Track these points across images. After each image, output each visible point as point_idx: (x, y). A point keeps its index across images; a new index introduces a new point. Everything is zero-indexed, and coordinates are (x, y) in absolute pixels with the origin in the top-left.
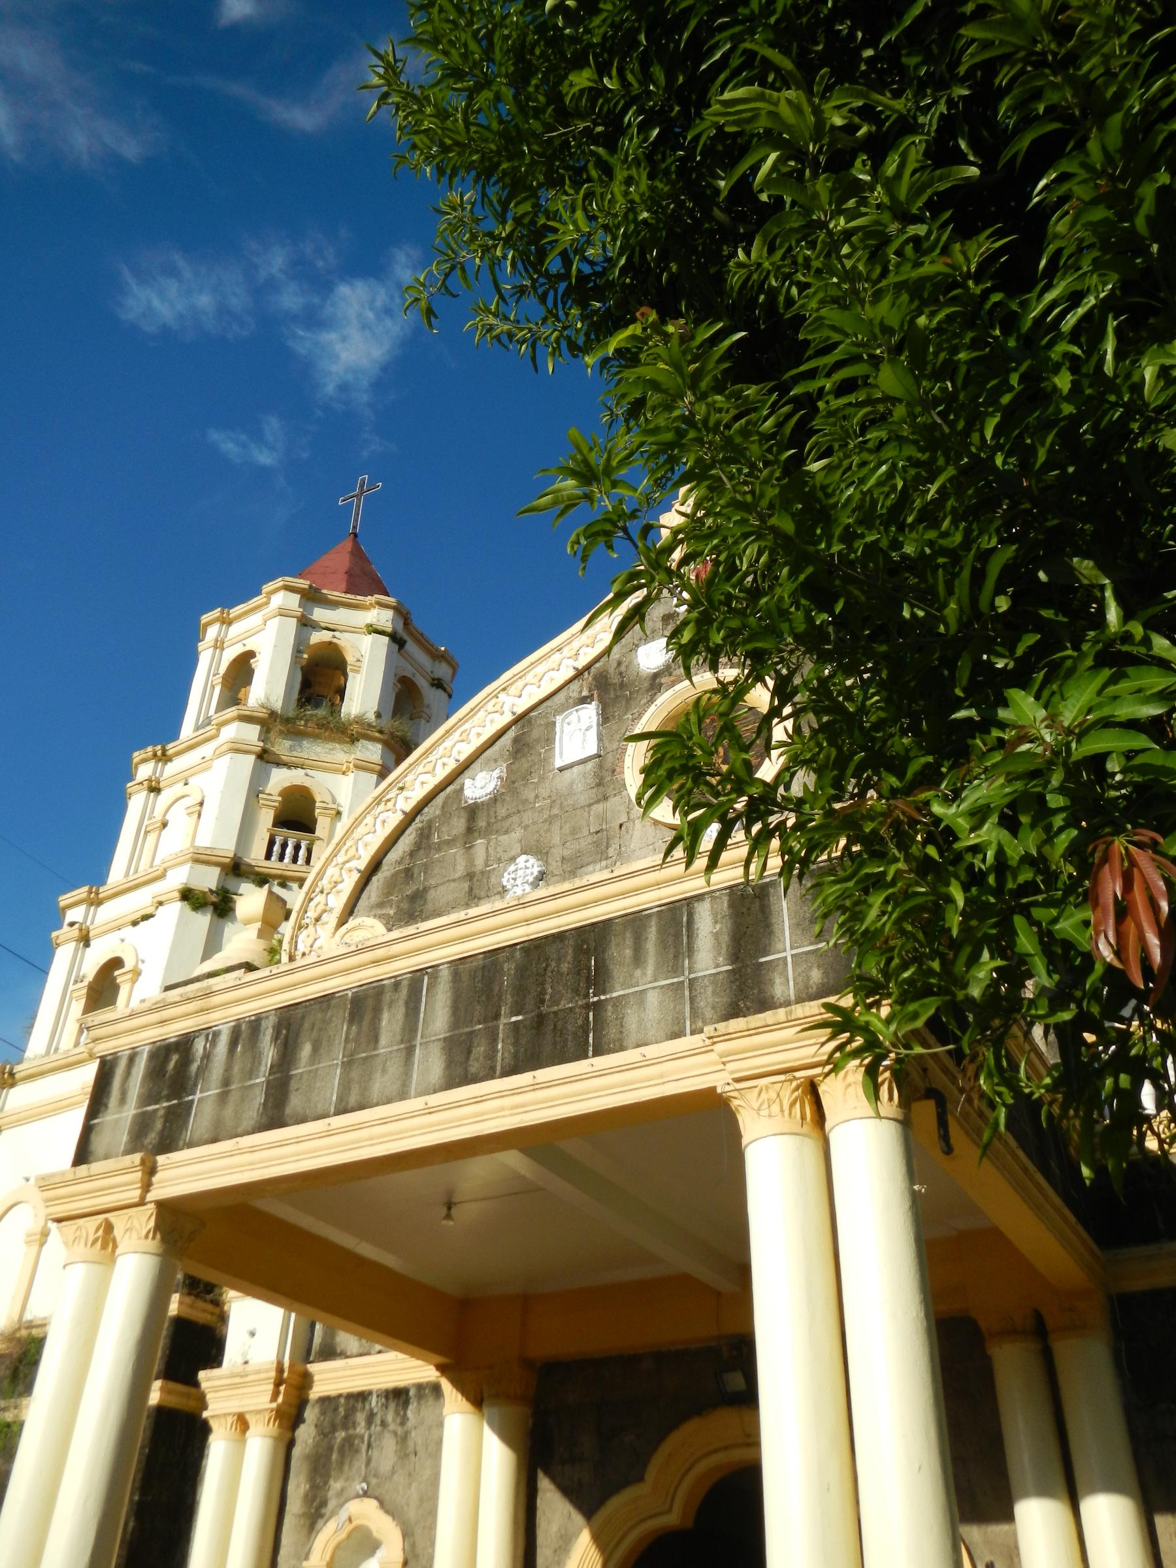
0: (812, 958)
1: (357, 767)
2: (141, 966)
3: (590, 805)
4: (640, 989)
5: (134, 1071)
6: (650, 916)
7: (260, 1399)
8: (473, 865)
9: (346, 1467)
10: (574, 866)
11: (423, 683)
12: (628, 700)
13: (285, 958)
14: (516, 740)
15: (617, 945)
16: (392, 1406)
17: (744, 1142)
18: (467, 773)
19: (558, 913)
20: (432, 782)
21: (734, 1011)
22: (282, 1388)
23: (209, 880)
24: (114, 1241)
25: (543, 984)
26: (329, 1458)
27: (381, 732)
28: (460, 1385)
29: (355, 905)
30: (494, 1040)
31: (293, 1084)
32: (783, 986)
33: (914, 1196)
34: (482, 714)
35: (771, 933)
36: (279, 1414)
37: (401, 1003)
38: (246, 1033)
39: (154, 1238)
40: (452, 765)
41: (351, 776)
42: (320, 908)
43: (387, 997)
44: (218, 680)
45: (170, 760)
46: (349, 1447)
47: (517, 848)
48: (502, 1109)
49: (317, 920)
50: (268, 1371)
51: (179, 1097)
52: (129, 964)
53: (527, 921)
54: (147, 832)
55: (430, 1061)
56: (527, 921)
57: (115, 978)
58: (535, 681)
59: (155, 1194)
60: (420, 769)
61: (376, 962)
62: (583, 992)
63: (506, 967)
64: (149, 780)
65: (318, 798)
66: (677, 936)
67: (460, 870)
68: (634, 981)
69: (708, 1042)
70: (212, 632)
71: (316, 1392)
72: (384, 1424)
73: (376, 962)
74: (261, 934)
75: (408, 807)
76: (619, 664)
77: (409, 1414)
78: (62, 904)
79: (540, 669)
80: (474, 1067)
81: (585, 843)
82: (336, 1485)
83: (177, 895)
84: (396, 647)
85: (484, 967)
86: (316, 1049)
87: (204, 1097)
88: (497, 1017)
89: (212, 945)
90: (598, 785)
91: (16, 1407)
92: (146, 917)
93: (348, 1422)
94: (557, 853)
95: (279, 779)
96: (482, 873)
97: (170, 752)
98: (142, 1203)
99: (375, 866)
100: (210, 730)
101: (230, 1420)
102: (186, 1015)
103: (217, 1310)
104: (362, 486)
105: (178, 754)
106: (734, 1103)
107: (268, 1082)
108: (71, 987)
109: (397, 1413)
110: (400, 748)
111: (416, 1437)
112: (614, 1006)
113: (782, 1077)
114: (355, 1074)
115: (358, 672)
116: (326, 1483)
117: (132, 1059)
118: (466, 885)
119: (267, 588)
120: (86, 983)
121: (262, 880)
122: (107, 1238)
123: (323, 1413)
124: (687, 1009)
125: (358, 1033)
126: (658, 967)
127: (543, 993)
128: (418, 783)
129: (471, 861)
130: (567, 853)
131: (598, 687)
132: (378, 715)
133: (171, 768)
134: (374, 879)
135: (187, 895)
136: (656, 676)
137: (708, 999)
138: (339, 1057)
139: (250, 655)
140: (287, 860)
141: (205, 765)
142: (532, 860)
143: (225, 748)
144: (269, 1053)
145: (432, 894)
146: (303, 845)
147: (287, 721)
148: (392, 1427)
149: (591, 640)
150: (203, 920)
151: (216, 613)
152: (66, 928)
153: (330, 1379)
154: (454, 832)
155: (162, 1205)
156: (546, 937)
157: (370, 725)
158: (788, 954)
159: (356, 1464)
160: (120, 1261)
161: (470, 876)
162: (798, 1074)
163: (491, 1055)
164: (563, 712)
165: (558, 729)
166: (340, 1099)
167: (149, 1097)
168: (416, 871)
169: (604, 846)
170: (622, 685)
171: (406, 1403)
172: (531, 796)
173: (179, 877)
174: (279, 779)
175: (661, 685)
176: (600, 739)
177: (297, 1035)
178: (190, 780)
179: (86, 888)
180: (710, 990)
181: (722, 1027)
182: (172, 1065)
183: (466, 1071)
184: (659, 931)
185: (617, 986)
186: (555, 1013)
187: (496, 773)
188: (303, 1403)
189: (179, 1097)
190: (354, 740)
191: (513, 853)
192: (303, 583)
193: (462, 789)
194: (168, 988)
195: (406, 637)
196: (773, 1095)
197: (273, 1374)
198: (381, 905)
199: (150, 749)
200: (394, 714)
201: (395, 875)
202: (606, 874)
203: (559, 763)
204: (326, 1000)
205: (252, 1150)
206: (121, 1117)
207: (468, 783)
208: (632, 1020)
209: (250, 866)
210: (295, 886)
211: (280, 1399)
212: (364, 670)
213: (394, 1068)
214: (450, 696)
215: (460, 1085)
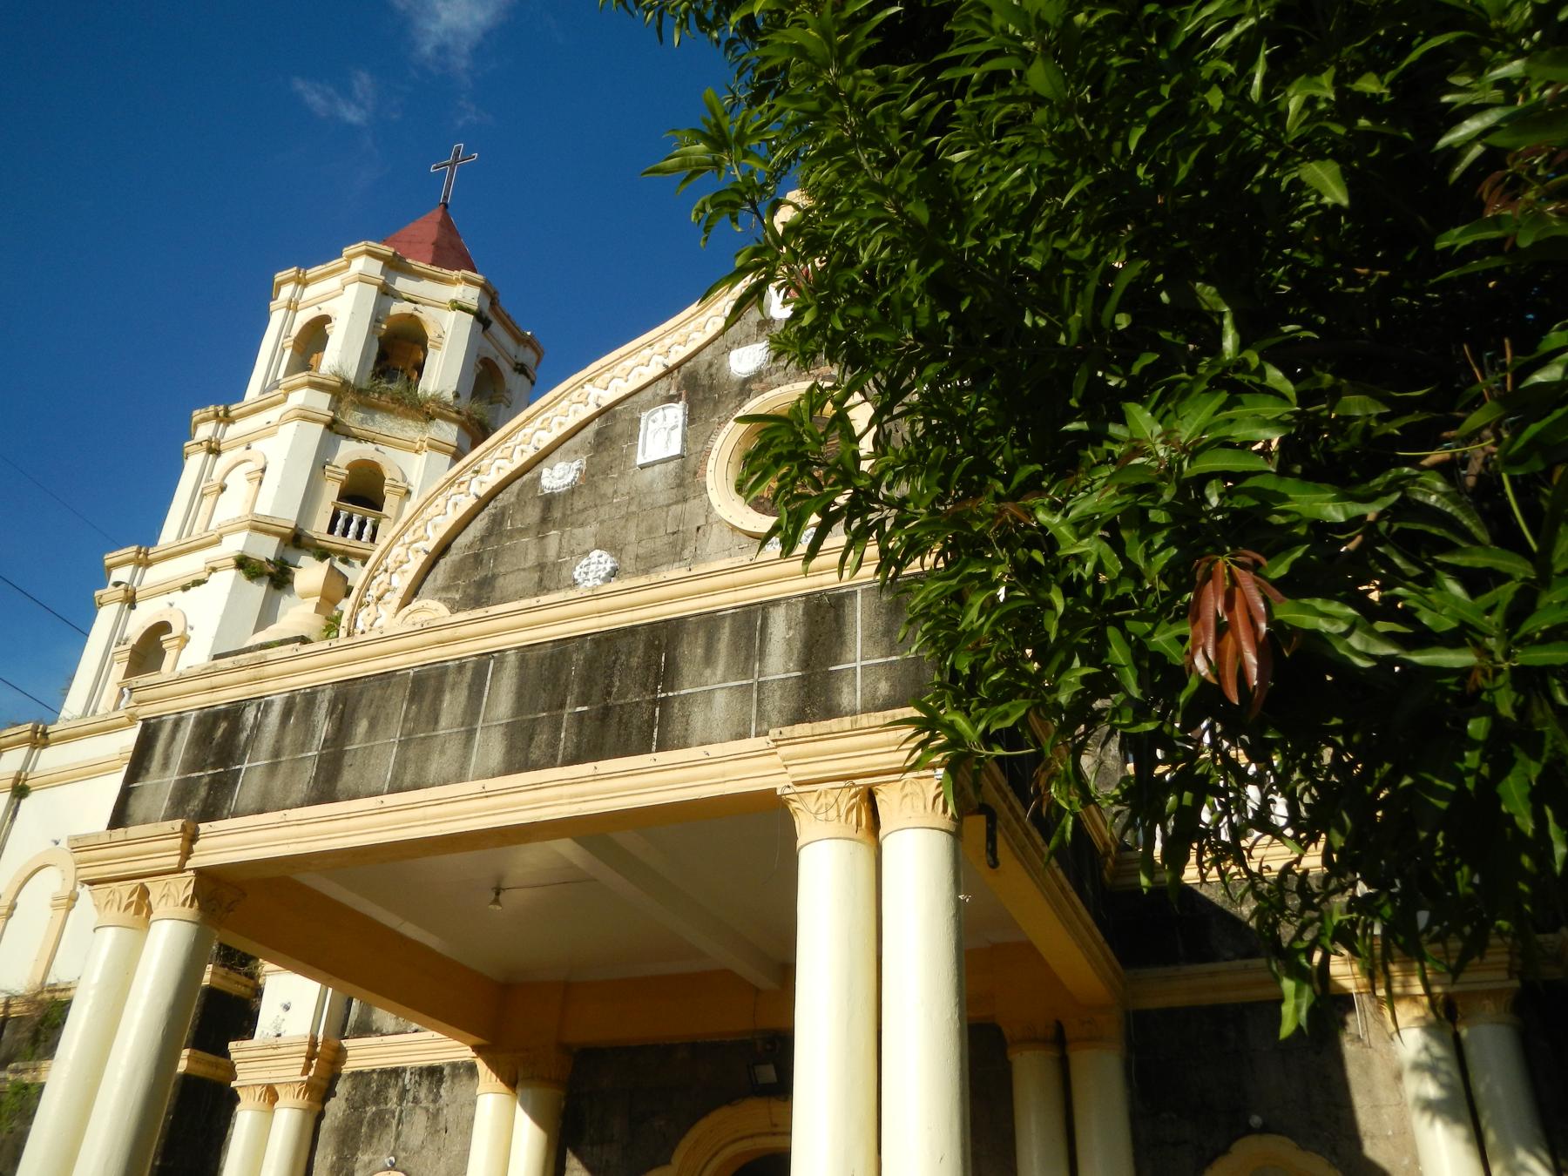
0: (881, 671)
1: (430, 446)
2: (189, 632)
3: (669, 505)
4: (710, 688)
5: (179, 736)
6: (724, 617)
7: (291, 1072)
8: (544, 555)
9: (375, 1140)
10: (648, 564)
11: (505, 367)
12: (716, 403)
13: (343, 633)
14: (598, 433)
15: (689, 644)
16: (426, 1083)
17: (799, 844)
18: (545, 462)
19: (632, 607)
20: (509, 468)
21: (799, 717)
22: (314, 1062)
23: (267, 549)
24: (149, 905)
25: (611, 676)
26: (358, 1131)
27: (458, 412)
28: (491, 1064)
29: (419, 587)
30: (558, 729)
31: (347, 760)
32: (850, 696)
33: (959, 905)
34: (565, 403)
35: (843, 643)
36: (310, 1087)
37: (465, 685)
38: (300, 705)
39: (191, 906)
40: (531, 453)
41: (425, 455)
42: (382, 588)
43: (450, 679)
44: (289, 342)
45: (233, 422)
46: (380, 1121)
47: (591, 542)
48: (561, 797)
49: (379, 599)
50: (300, 1044)
51: (226, 766)
52: (177, 630)
53: (600, 613)
54: (203, 495)
55: (489, 746)
56: (600, 613)
57: (161, 643)
58: (624, 374)
59: (195, 861)
60: (498, 454)
61: (441, 643)
62: (651, 687)
63: (575, 657)
64: (209, 441)
65: (387, 475)
66: (751, 638)
67: (532, 559)
68: (703, 680)
69: (772, 745)
70: (286, 292)
71: (350, 1066)
72: (416, 1100)
73: (441, 643)
74: (319, 609)
75: (482, 492)
76: (710, 365)
77: (442, 1091)
78: (108, 562)
79: (629, 363)
80: (535, 754)
81: (660, 542)
82: (364, 1158)
83: (232, 562)
84: (481, 327)
85: (552, 655)
87: (252, 768)
88: (562, 706)
89: (266, 616)
90: (679, 486)
91: (35, 1069)
92: (197, 583)
93: (380, 1096)
94: (632, 550)
95: (348, 452)
96: (554, 564)
97: (232, 414)
98: (181, 869)
99: (443, 548)
100: (278, 394)
101: (258, 1090)
102: (238, 683)
103: (251, 983)
104: (457, 155)
105: (242, 416)
106: (793, 805)
107: (321, 756)
108: (113, 649)
109: (430, 1090)
110: (477, 431)
111: (448, 1114)
112: (682, 703)
113: (842, 784)
114: (411, 754)
115: (438, 348)
116: (353, 1155)
117: (177, 724)
118: (536, 576)
119: (348, 251)
120: (129, 646)
121: (323, 554)
122: (142, 904)
123: (355, 1088)
124: (754, 711)
125: (419, 712)
126: (728, 667)
127: (610, 685)
128: (494, 468)
129: (543, 551)
130: (641, 551)
131: (687, 387)
132: (457, 395)
133: (233, 431)
134: (442, 562)
135: (242, 563)
136: (746, 381)
137: (776, 702)
138: (396, 735)
139: (326, 319)
140: (350, 536)
141: (270, 430)
142: (606, 556)
143: (291, 414)
145: (500, 582)
146: (369, 521)
147: (360, 391)
148: (424, 1104)
149: (682, 339)
150: (259, 590)
151: (292, 272)
152: (110, 587)
153: (363, 1054)
154: (528, 521)
155: (200, 872)
156: (618, 630)
157: (447, 405)
158: (858, 664)
159: (386, 1138)
160: (154, 926)
161: (541, 567)
162: (857, 782)
163: (553, 744)
164: (648, 408)
165: (642, 426)
166: (395, 777)
167: (193, 764)
168: (486, 557)
169: (679, 546)
170: (711, 388)
171: (440, 1081)
172: (610, 491)
173: (235, 544)
174: (348, 452)
175: (751, 391)
176: (684, 439)
177: (354, 710)
178: (253, 445)
179: (135, 548)
180: (778, 694)
181: (787, 731)
182: (220, 732)
183: (527, 758)
184: (732, 633)
185: (686, 684)
186: (621, 706)
187: (576, 465)
188: (334, 1077)
189: (226, 766)
190: (430, 418)
191: (587, 547)
192: (387, 250)
193: (539, 477)
194: (216, 657)
195: (491, 317)
196: (832, 800)
197: (306, 1048)
198: (446, 589)
199: (211, 408)
200: (474, 395)
202: (683, 572)
203: (640, 460)
204: (387, 677)
205: (300, 823)
206: (162, 782)
207: (546, 472)
208: (698, 720)
209: (311, 538)
210: (357, 563)
211: (311, 1073)
212: (445, 347)
213: (453, 749)
214: (533, 383)
215: (520, 771)
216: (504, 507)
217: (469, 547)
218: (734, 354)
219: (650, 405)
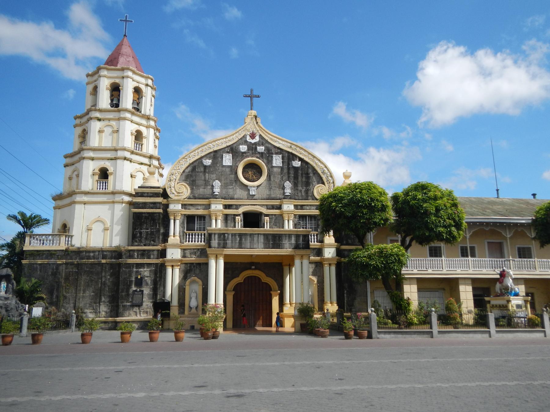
14: (214, 155)
38: (234, 235)
55: (261, 245)
60: (192, 154)
67: (203, 178)
86: (245, 240)
87: (229, 242)
92: (111, 159)
94: (223, 182)
129: (205, 178)
136: (243, 153)
138: (248, 241)
144: (238, 239)
145: (197, 182)
167: (218, 240)
201: (188, 175)
213: (257, 244)
216: (195, 166)
217: (189, 172)
218: (241, 146)
219: (224, 152)
